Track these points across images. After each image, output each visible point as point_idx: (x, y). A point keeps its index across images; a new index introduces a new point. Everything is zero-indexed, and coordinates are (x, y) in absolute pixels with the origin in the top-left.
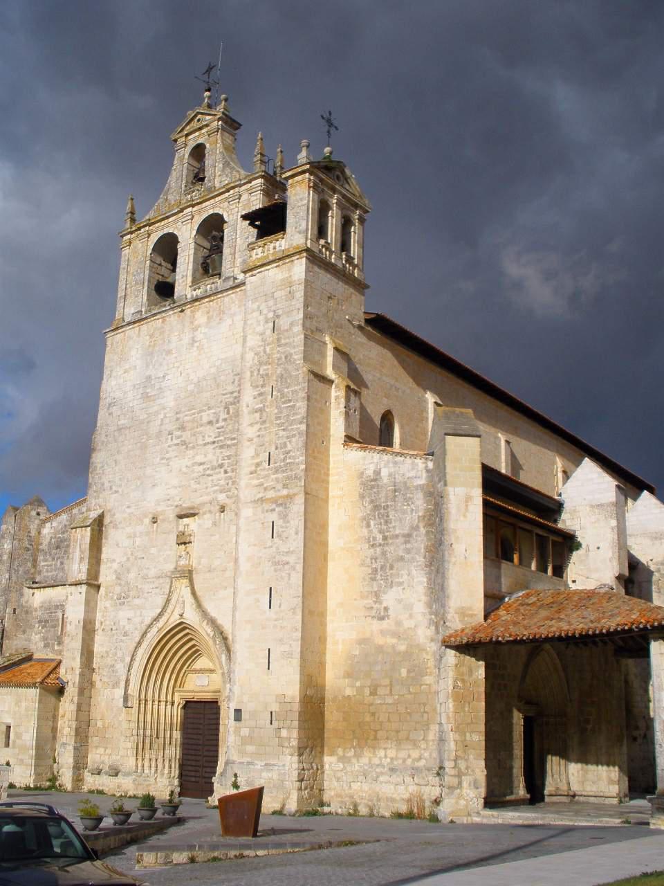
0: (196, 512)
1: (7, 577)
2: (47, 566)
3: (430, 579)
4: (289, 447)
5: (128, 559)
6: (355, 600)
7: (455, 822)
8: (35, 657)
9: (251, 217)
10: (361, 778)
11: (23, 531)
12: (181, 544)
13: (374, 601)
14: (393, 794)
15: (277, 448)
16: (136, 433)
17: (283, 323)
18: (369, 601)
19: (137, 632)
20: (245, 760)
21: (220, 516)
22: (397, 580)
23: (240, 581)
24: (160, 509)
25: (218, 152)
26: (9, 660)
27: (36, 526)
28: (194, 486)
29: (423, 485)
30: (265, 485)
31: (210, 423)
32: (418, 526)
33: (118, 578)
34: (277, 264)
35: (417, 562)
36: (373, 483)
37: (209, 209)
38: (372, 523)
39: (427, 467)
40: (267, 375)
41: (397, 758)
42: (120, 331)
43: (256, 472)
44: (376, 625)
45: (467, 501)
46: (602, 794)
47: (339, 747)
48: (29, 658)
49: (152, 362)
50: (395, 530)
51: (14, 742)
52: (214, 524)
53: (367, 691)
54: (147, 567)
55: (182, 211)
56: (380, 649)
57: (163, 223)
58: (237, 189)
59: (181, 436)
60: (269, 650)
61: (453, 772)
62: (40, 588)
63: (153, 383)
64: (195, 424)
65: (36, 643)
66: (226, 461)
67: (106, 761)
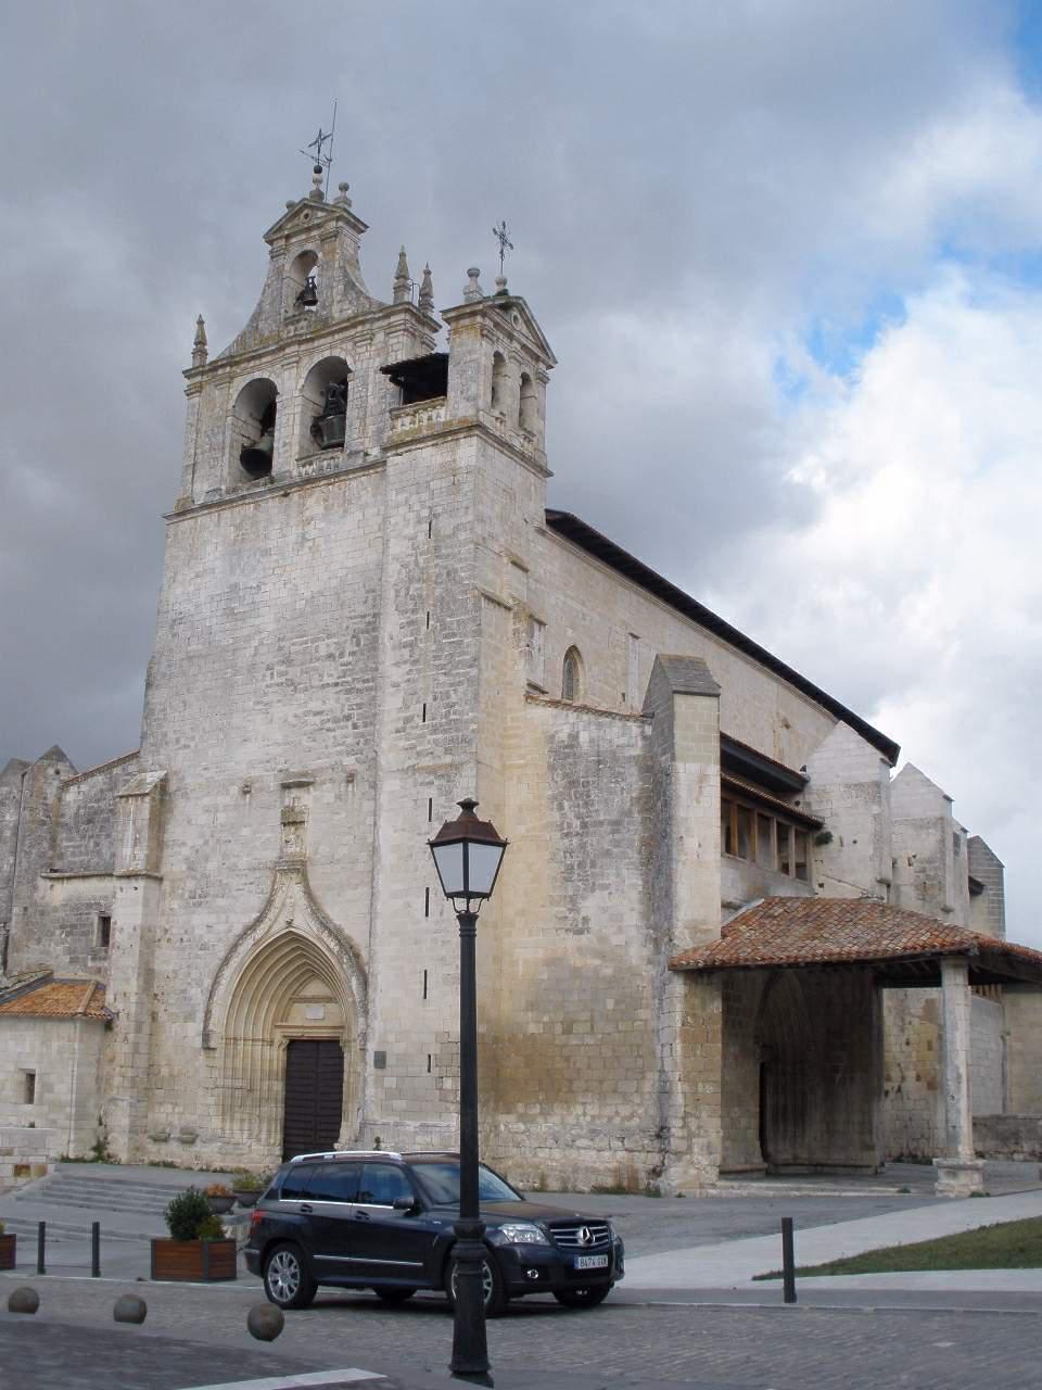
0: (312, 780)
1: (12, 861)
2: (73, 846)
3: (646, 882)
4: (454, 698)
5: (206, 843)
6: (543, 906)
7: (684, 1196)
8: (57, 975)
9: (395, 372)
10: (550, 1142)
11: (37, 797)
12: (289, 823)
13: (569, 909)
14: (595, 1162)
15: (435, 699)
16: (216, 666)
17: (445, 525)
18: (562, 909)
20: (391, 1120)
21: (347, 786)
22: (601, 882)
23: (382, 880)
24: (255, 773)
25: (337, 265)
26: (20, 982)
27: (54, 790)
28: (306, 743)
29: (639, 756)
30: (418, 749)
31: (330, 656)
32: (630, 811)
33: (190, 868)
34: (434, 442)
35: (630, 858)
36: (567, 751)
37: (324, 350)
38: (566, 804)
39: (643, 732)
40: (420, 596)
41: (599, 1117)
42: (189, 516)
43: (404, 730)
44: (571, 941)
45: (701, 781)
46: (852, 1162)
47: (519, 1101)
48: (47, 979)
49: (239, 565)
50: (599, 815)
51: (41, 1096)
52: (338, 797)
53: (559, 1029)
55: (282, 348)
56: (576, 972)
57: (252, 364)
58: (368, 326)
59: (287, 673)
60: (426, 972)
61: (680, 1133)
62: (62, 878)
63: (241, 594)
64: (308, 657)
65: (57, 957)
66: (355, 712)
67: (176, 1122)
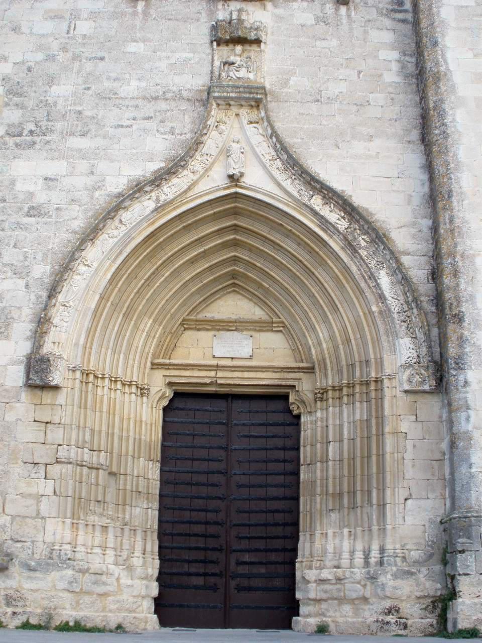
5: (51, 58)
54: (113, 75)
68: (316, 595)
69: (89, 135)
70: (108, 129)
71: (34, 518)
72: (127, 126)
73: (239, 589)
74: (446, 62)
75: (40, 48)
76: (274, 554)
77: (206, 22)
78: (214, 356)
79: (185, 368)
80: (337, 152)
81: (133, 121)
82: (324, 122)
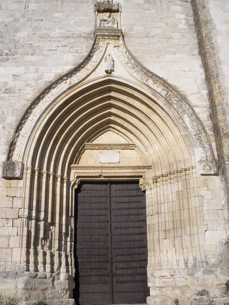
19: (29, 88)
54: (48, 27)
68: (160, 285)
69: (35, 54)
70: (45, 52)
71: (6, 248)
72: (54, 50)
73: (118, 282)
74: (210, 15)
75: (11, 16)
76: (135, 263)
77: (92, 3)
78: (101, 162)
79: (86, 168)
80: (158, 60)
81: (57, 48)
82: (151, 46)
